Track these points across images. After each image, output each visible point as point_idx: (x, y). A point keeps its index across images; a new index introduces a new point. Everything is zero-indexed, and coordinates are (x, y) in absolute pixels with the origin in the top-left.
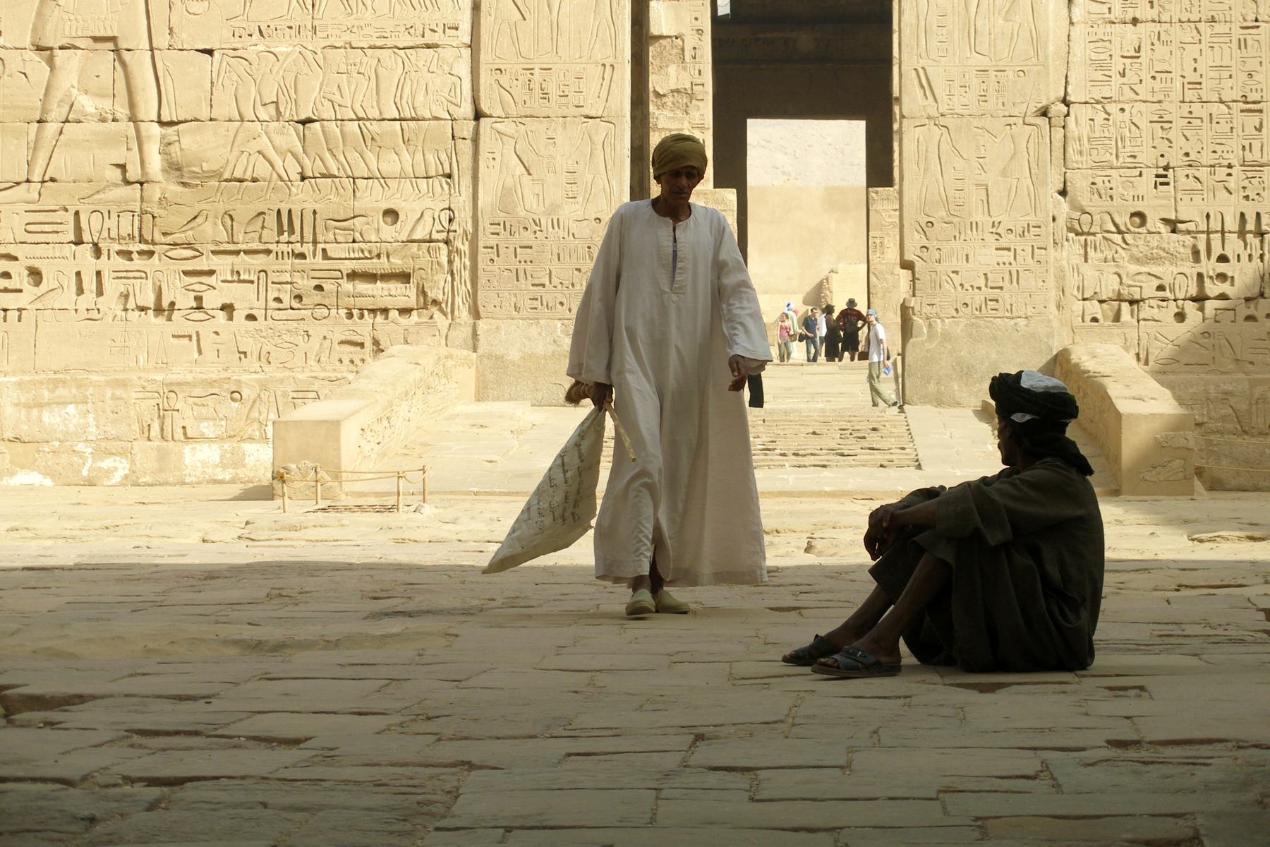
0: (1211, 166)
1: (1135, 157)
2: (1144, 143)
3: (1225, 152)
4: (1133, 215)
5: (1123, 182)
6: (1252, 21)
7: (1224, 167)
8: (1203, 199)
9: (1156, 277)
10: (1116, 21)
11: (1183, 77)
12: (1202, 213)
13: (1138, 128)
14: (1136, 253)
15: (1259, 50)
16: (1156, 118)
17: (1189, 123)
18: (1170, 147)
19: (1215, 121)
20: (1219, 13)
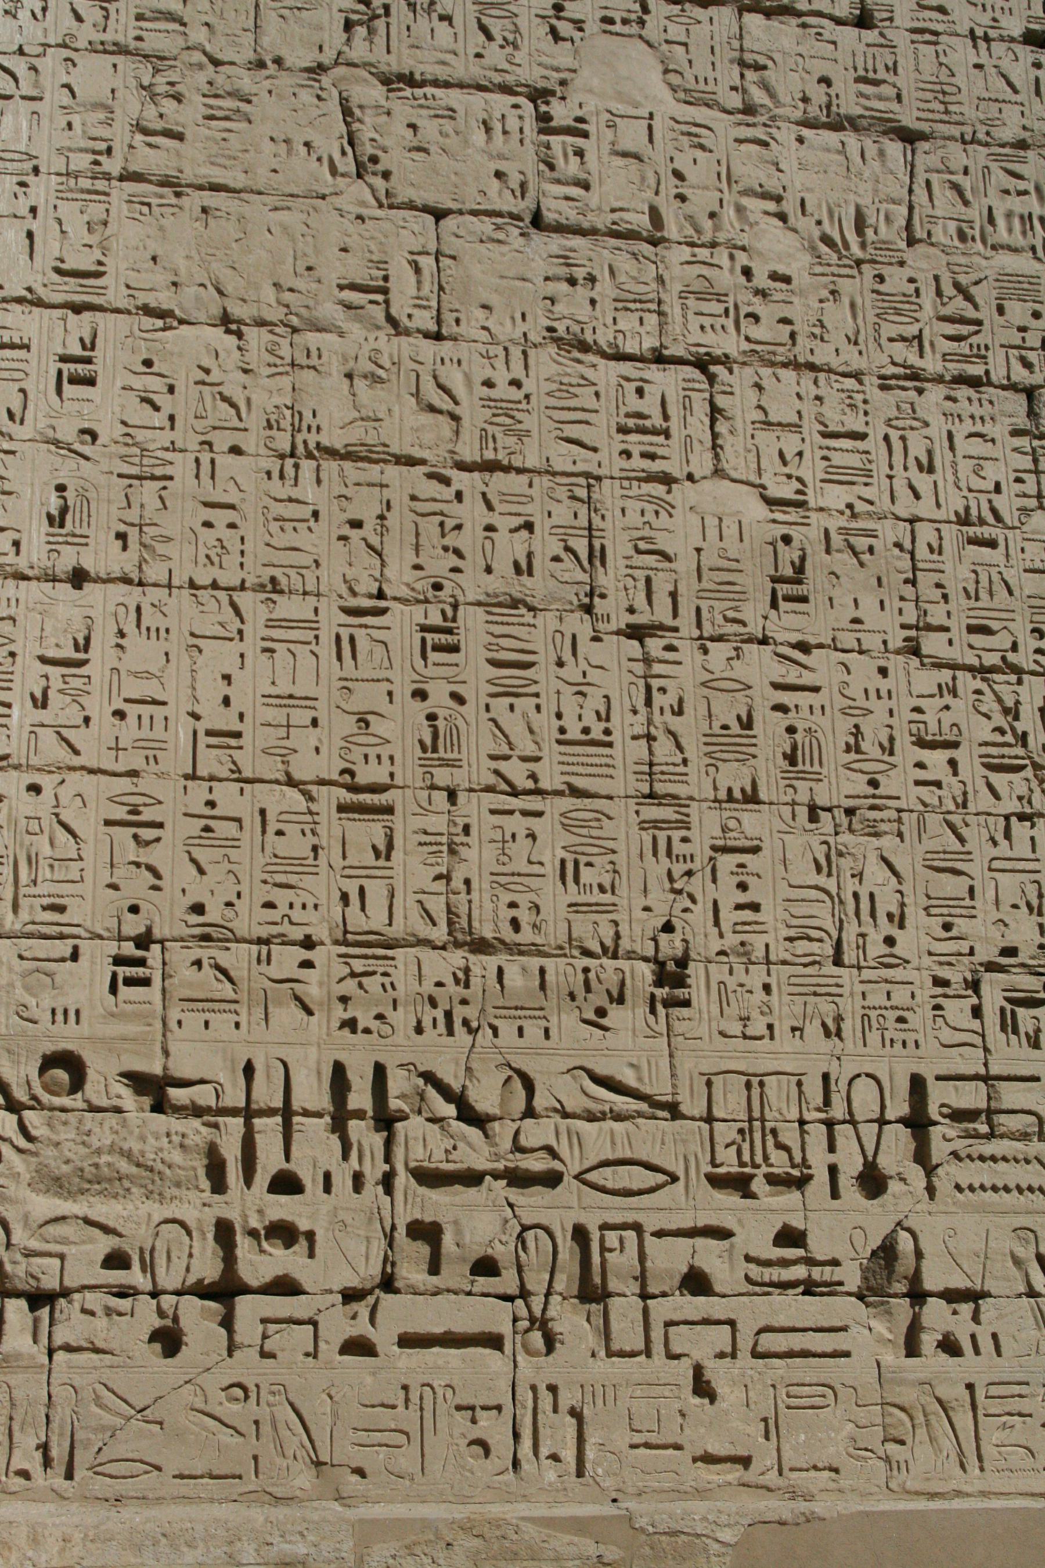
0: (260, 941)
1: (61, 909)
2: (88, 876)
3: (298, 906)
4: (50, 1062)
5: (26, 975)
6: (371, 596)
7: (293, 943)
8: (237, 1025)
9: (106, 1230)
10: (30, 573)
11: (196, 717)
12: (233, 1061)
13: (74, 835)
14: (53, 1164)
15: (386, 664)
16: (120, 813)
17: (207, 829)
18: (155, 888)
19: (272, 827)
20: (292, 572)
